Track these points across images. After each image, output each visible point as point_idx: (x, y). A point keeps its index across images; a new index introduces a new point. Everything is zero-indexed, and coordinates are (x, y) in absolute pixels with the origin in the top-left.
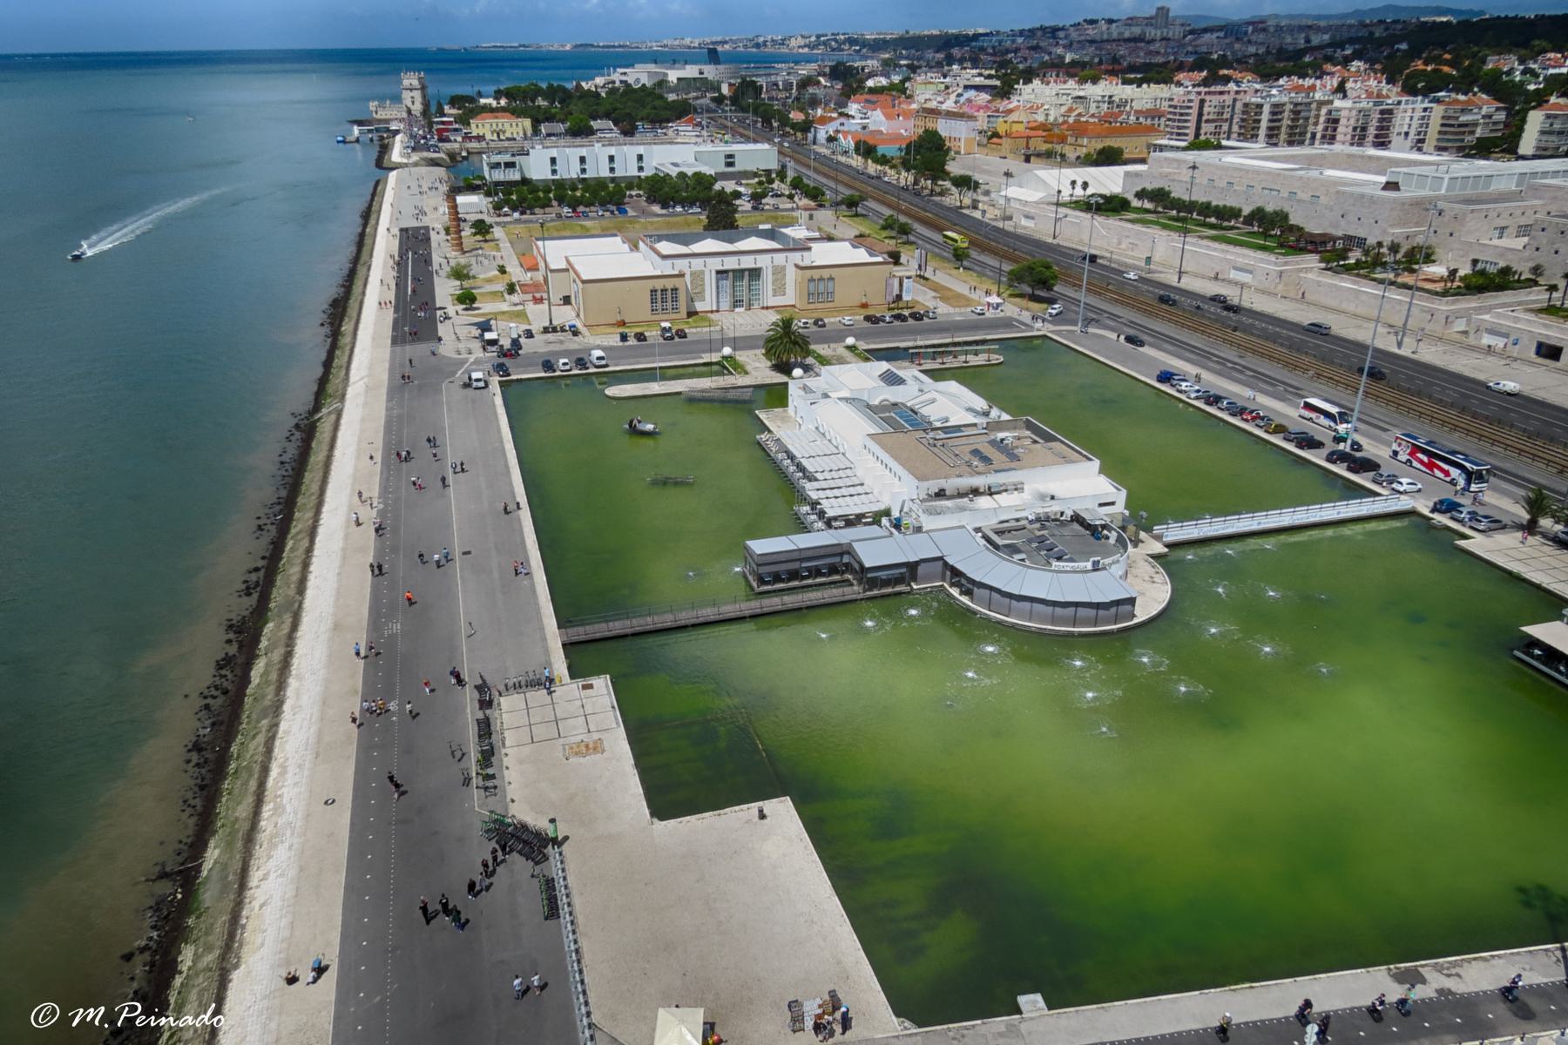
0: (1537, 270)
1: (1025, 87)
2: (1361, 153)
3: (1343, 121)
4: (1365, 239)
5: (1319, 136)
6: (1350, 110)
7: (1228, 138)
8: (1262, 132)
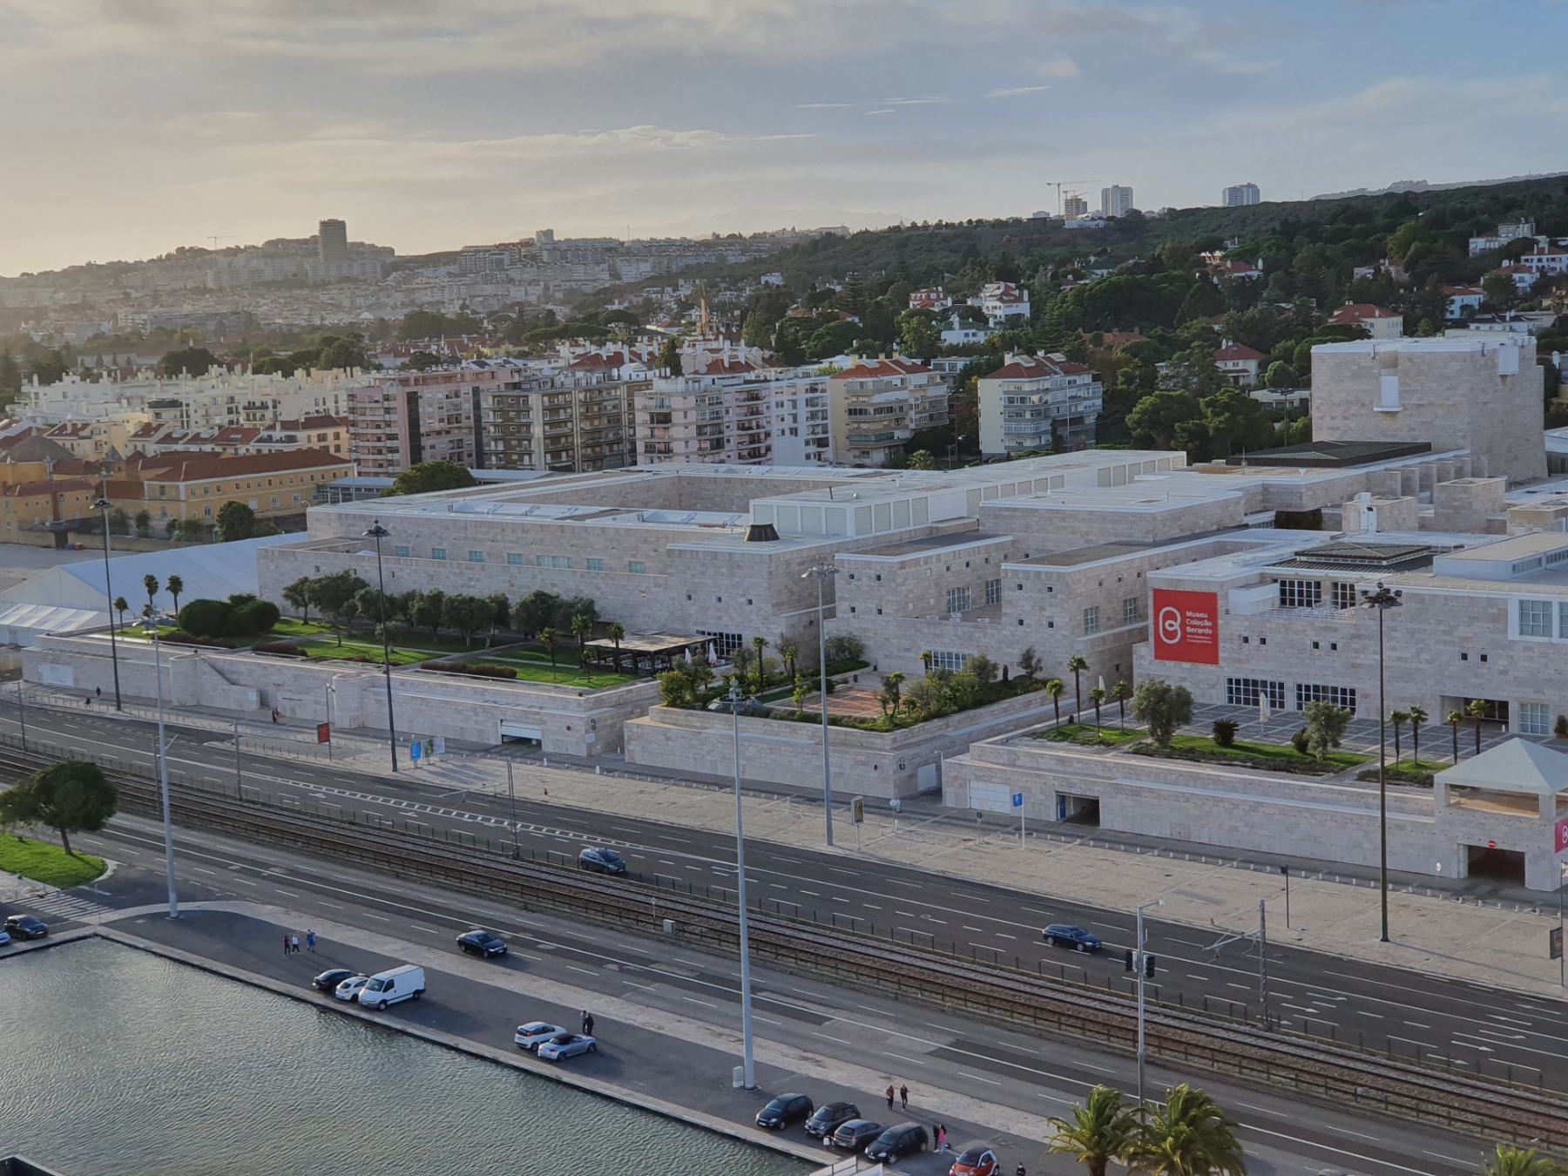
0: (1027, 659)
2: (713, 475)
3: (677, 417)
4: (740, 637)
5: (640, 447)
6: (685, 395)
7: (480, 466)
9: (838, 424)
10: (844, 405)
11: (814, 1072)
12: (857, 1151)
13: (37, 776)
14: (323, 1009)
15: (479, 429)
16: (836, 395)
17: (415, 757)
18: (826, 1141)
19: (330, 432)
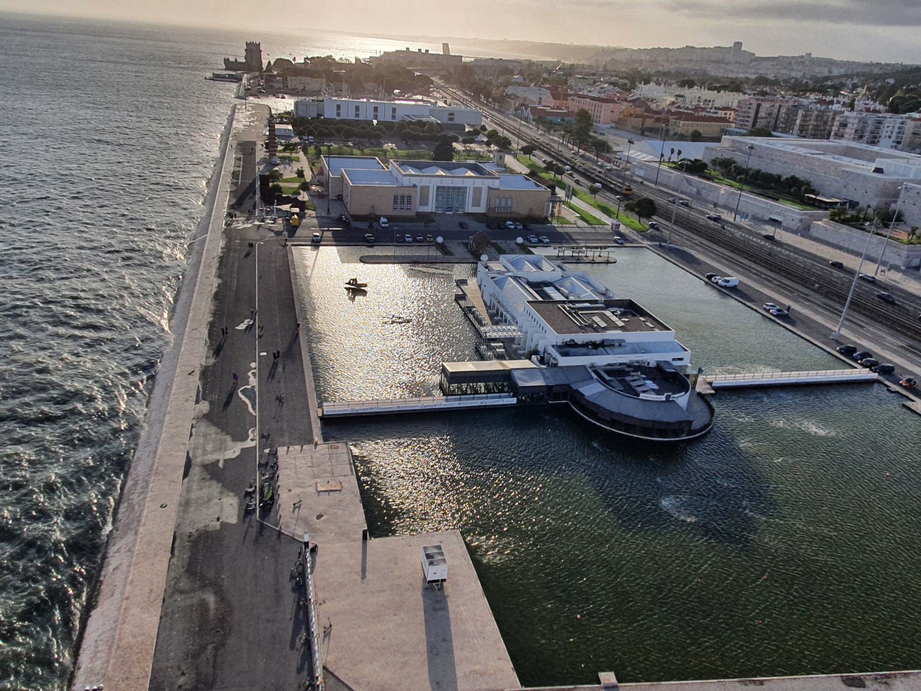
1: (644, 86)
3: (849, 126)
5: (833, 133)
6: (855, 118)
7: (774, 131)
8: (796, 128)
9: (907, 137)
10: (912, 130)
11: (858, 341)
12: (870, 367)
13: (637, 200)
14: (707, 283)
15: (777, 118)
16: (910, 126)
17: (741, 218)
18: (859, 361)
19: (728, 112)
